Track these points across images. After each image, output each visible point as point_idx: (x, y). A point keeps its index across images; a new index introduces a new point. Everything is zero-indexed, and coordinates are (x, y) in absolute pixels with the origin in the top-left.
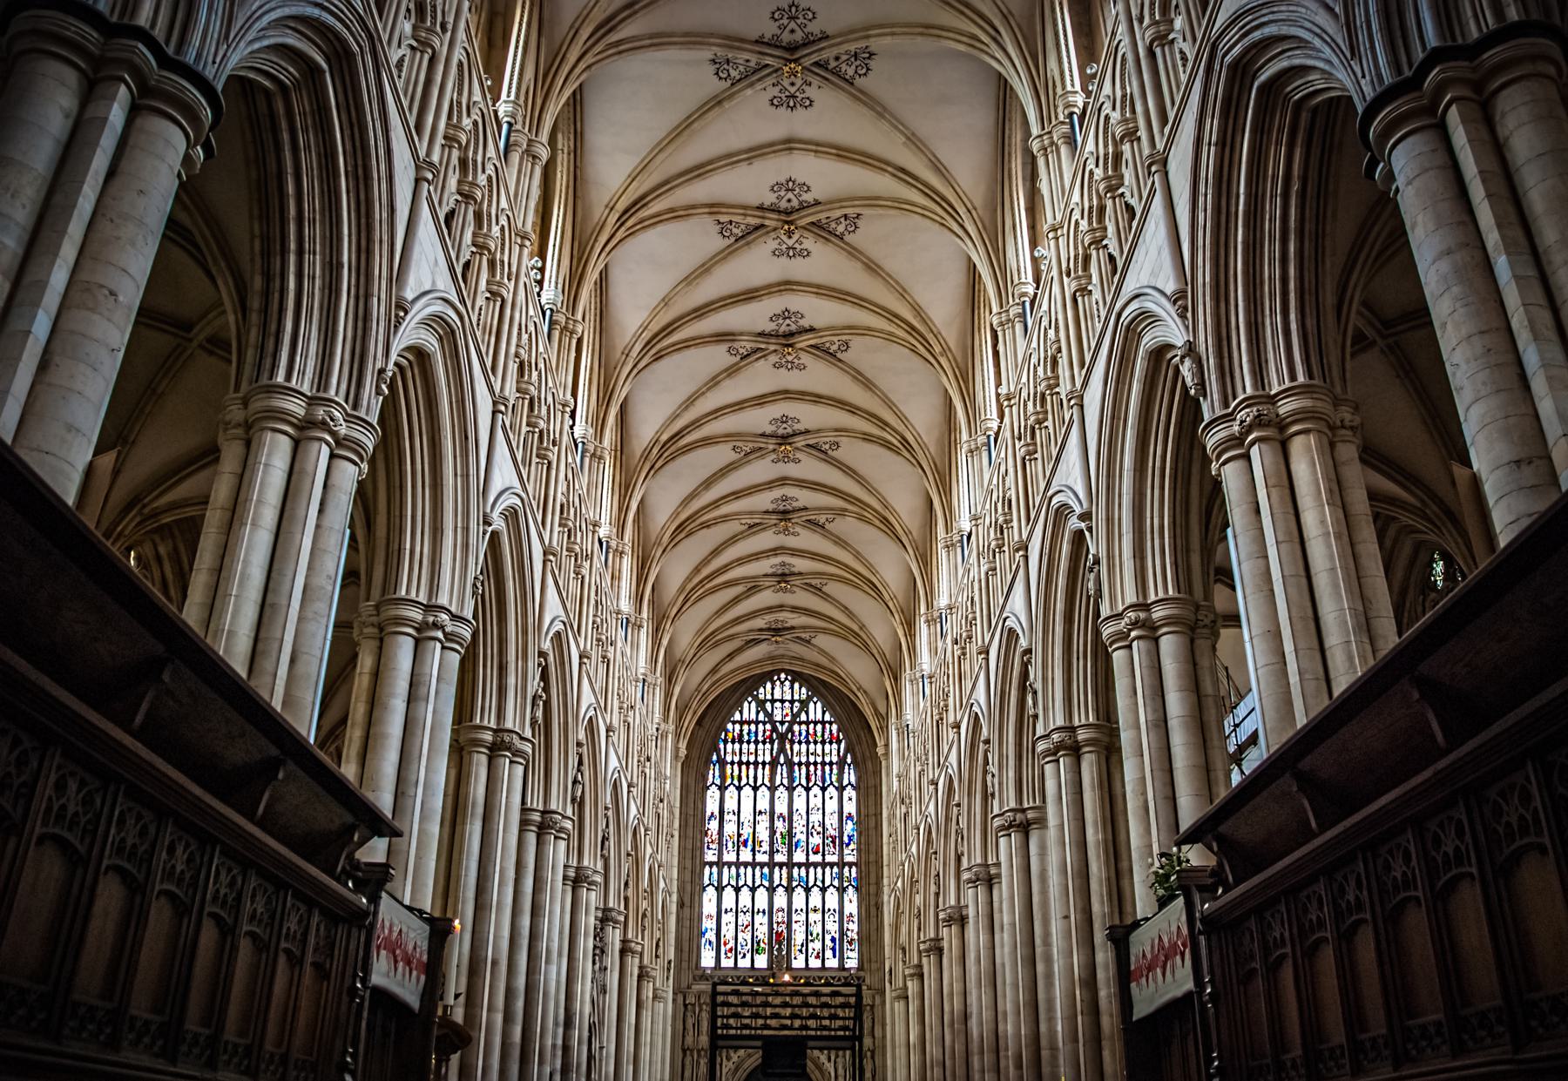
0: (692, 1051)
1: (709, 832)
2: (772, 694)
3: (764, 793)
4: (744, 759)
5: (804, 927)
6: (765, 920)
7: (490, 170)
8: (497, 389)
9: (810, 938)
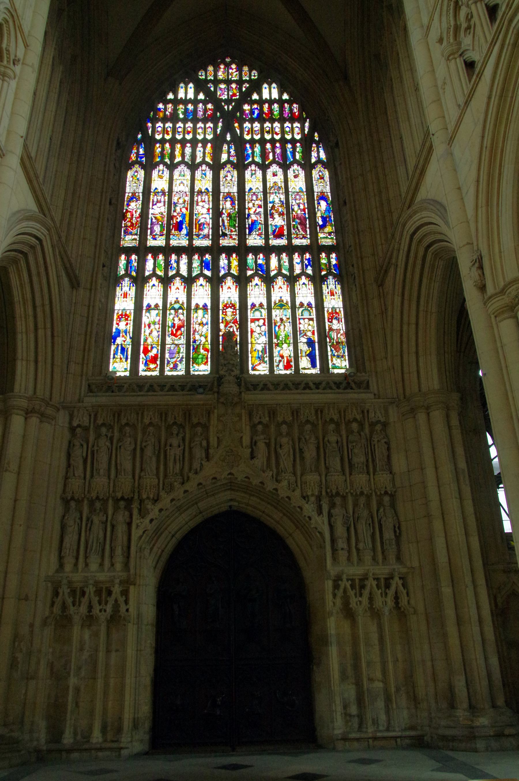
0: (79, 502)
1: (129, 215)
2: (215, 76)
4: (179, 137)
5: (265, 328)
6: (208, 318)
9: (275, 341)
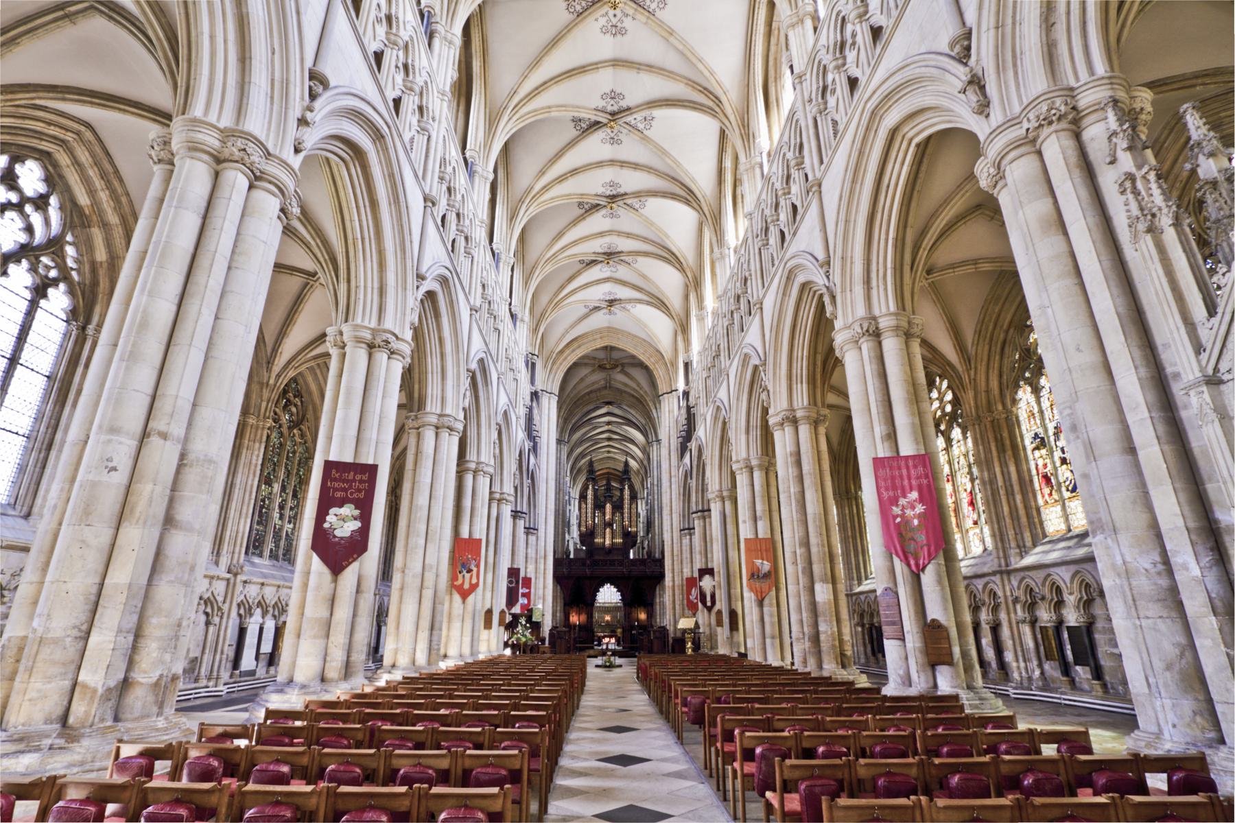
7: (463, 191)
8: (472, 303)
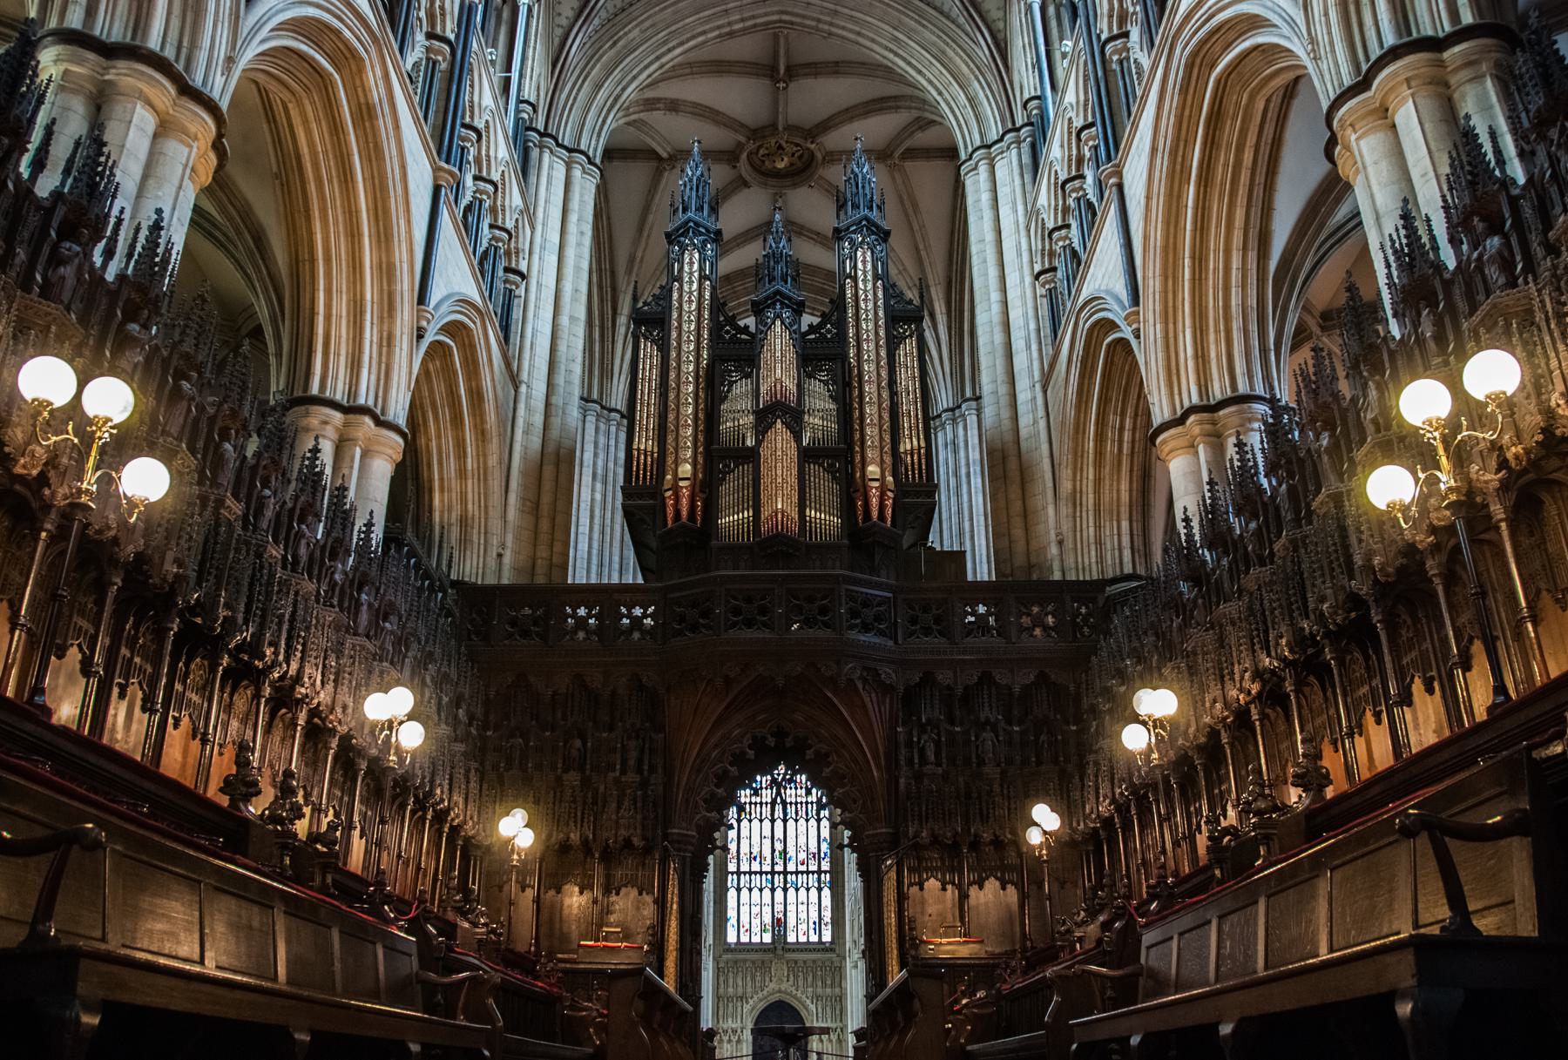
3: (767, 824)
